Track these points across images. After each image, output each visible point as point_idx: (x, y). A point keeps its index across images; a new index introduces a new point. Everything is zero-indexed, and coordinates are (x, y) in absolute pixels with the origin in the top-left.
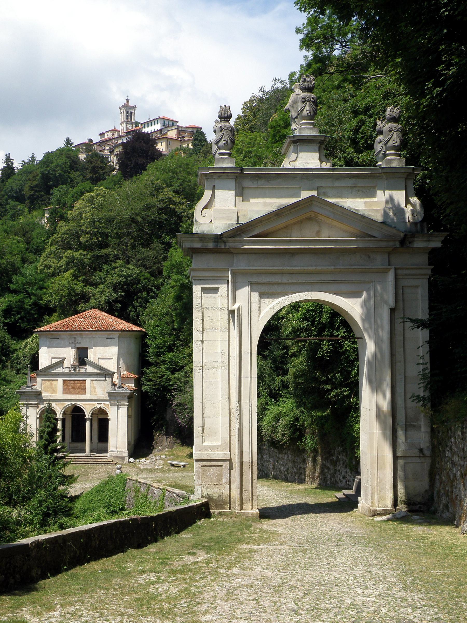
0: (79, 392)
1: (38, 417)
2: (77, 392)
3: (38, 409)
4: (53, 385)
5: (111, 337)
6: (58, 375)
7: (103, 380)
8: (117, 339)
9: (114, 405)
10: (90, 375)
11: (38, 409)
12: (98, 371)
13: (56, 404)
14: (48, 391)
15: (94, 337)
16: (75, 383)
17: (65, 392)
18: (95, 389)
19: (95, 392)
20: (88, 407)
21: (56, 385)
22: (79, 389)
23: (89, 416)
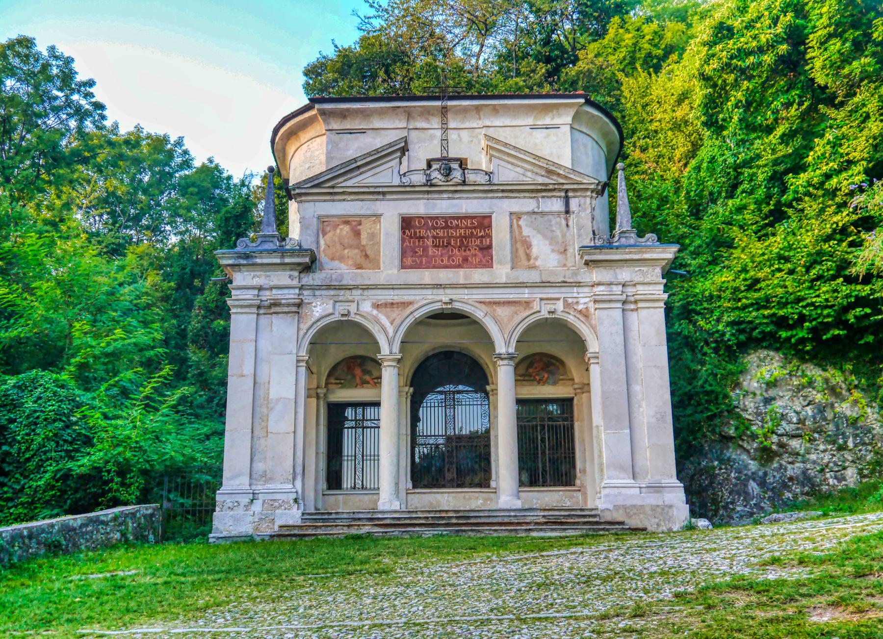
0: (465, 260)
1: (303, 353)
2: (458, 260)
3: (304, 327)
4: (364, 236)
5: (548, 121)
6: (380, 193)
7: (558, 213)
8: (567, 128)
9: (610, 301)
10: (510, 191)
11: (304, 327)
12: (540, 180)
13: (377, 306)
14: (341, 259)
15: (488, 123)
16: (447, 227)
17: (409, 261)
18: (528, 245)
19: (528, 257)
20: (503, 312)
21: (373, 236)
22: (463, 247)
23: (512, 350)
